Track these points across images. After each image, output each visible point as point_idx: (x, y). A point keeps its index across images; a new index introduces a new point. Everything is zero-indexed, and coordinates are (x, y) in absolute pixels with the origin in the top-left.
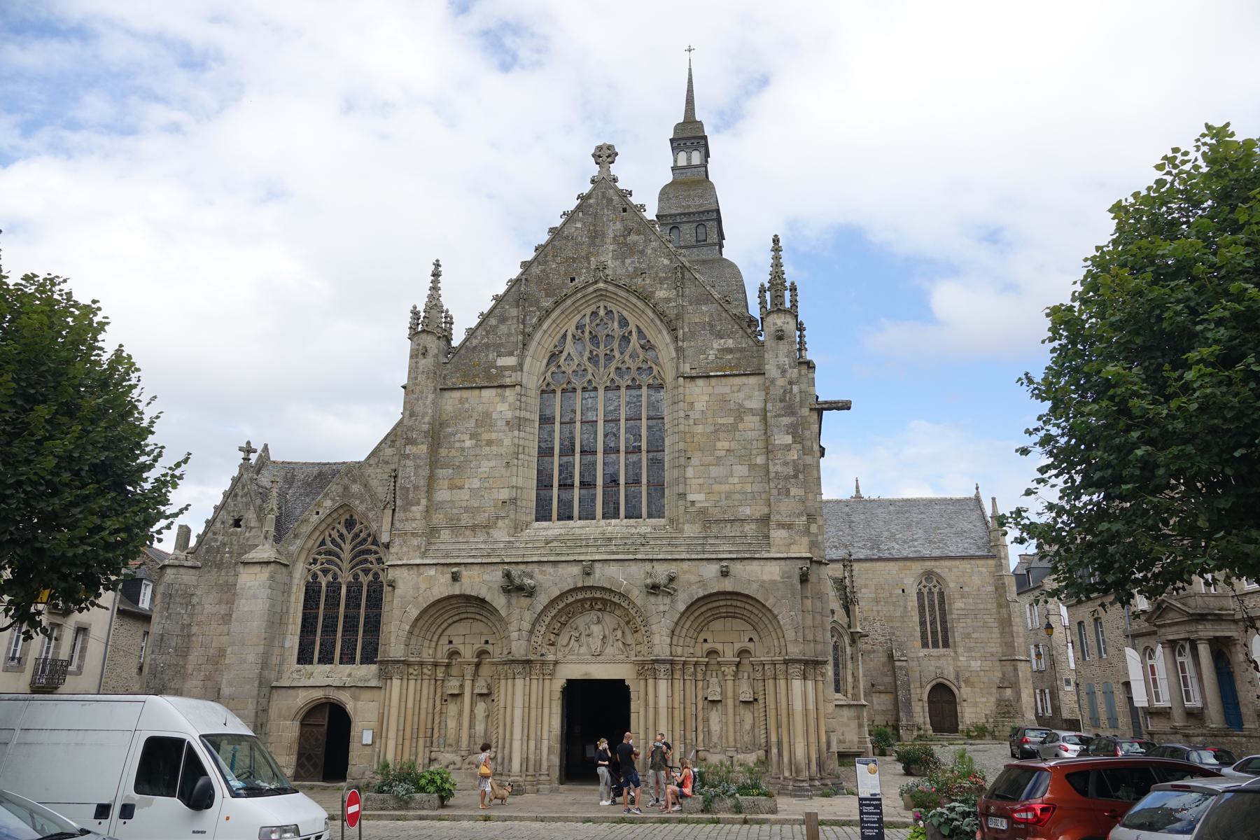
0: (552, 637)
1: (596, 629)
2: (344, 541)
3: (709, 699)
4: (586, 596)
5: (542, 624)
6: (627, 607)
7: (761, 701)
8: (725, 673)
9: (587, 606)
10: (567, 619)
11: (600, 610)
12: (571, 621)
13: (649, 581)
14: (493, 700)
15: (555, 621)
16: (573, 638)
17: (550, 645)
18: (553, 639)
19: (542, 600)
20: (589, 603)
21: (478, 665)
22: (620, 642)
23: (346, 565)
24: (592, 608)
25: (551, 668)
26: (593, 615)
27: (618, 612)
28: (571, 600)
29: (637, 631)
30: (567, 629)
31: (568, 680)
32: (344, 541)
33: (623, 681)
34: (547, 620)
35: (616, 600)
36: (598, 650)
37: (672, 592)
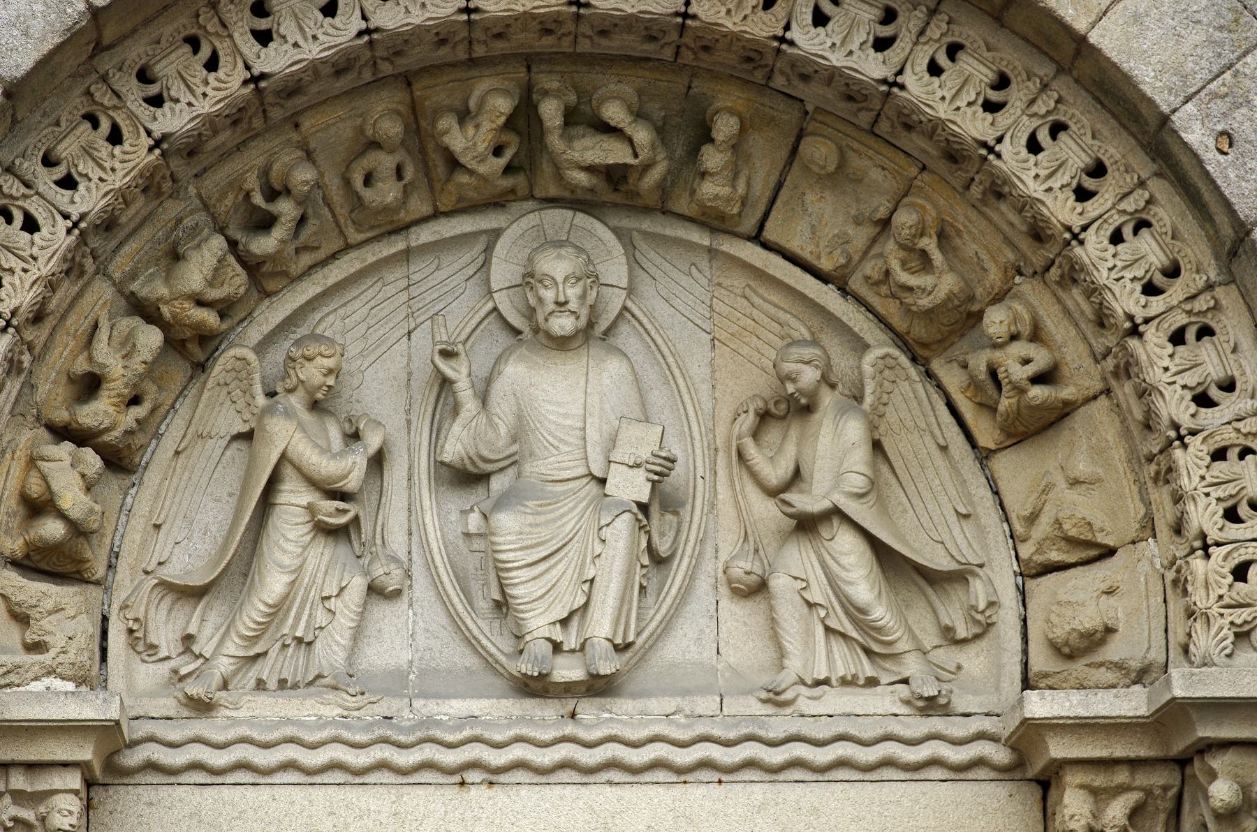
6: (975, 126)
10: (236, 281)
12: (271, 315)
15: (101, 294)
16: (294, 496)
18: (72, 498)
20: (503, 105)
29: (1062, 413)
36: (601, 625)
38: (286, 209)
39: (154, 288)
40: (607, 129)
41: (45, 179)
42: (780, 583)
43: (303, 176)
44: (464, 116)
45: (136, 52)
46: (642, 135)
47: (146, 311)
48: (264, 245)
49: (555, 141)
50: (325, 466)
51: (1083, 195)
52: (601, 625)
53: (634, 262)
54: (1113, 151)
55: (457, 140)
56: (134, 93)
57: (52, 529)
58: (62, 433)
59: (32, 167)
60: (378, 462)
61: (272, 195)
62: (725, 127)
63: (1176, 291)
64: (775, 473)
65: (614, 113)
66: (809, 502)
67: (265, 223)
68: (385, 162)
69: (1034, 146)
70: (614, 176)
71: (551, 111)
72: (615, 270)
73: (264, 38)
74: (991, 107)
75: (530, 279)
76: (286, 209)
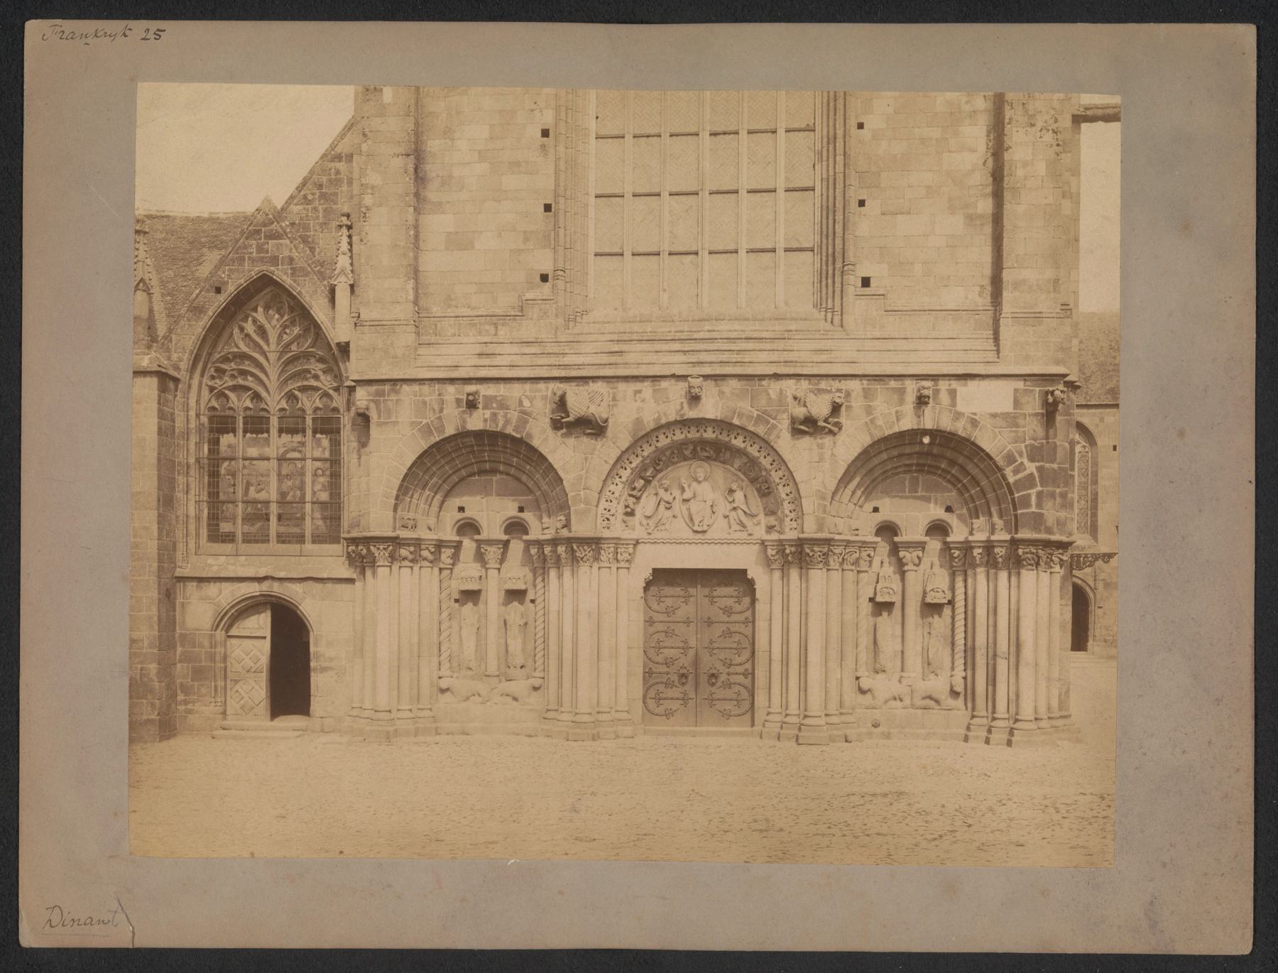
0: (631, 500)
1: (705, 490)
2: (267, 341)
3: (879, 599)
4: (689, 436)
5: (617, 480)
7: (960, 603)
8: (904, 561)
9: (687, 453)
11: (708, 458)
12: (659, 476)
13: (800, 412)
14: (533, 601)
17: (627, 514)
18: (632, 506)
19: (619, 437)
21: (506, 544)
22: (740, 512)
23: (273, 380)
24: (695, 456)
25: (631, 550)
26: (701, 469)
27: (737, 463)
28: (664, 441)
30: (650, 490)
31: (655, 570)
32: (267, 341)
33: (744, 572)
34: (626, 474)
35: (738, 442)
37: (836, 429)
38: (661, 463)
39: (643, 475)
40: (707, 451)
41: (627, 462)
42: (731, 517)
43: (664, 459)
44: (686, 449)
45: (640, 444)
46: (712, 452)
47: (642, 478)
48: (658, 468)
49: (700, 453)
50: (666, 499)
51: (772, 464)
52: (706, 522)
53: (711, 468)
54: (776, 458)
55: (687, 453)
56: (639, 449)
57: (629, 510)
58: (630, 495)
59: (626, 461)
60: (674, 498)
61: (659, 460)
62: (723, 450)
63: (784, 479)
64: (731, 499)
65: (707, 449)
66: (735, 505)
67: (659, 464)
68: (675, 456)
69: (765, 457)
70: (708, 457)
71: (699, 449)
72: (709, 470)
73: (658, 441)
74: (759, 451)
75: (695, 472)
76: (661, 463)
